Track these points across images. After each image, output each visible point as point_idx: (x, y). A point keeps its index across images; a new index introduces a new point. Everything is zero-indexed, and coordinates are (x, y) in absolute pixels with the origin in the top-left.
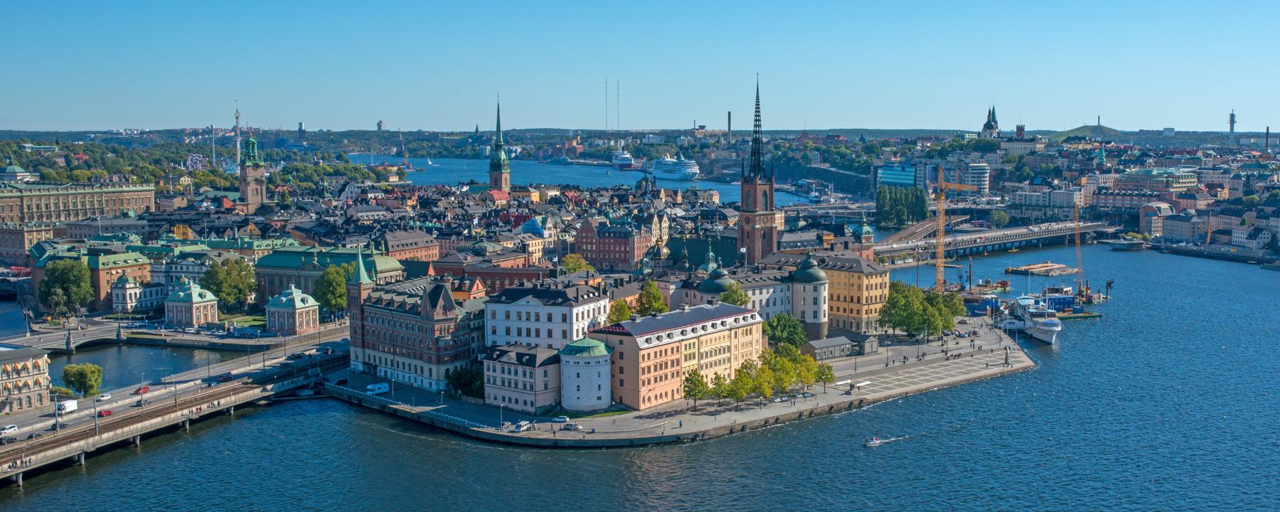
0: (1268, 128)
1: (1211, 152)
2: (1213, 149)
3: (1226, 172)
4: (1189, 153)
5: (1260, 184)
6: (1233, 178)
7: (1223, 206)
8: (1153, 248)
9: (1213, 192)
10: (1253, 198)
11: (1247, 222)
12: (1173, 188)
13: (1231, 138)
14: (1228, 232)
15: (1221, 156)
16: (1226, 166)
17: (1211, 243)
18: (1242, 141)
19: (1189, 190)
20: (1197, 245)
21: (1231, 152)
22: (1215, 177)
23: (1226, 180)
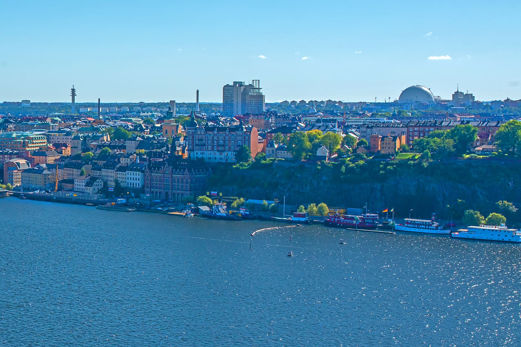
0: (99, 99)
1: (57, 118)
2: (59, 116)
3: (68, 134)
4: (40, 119)
5: (94, 143)
6: (74, 139)
7: (67, 161)
8: (15, 195)
9: (59, 150)
10: (89, 154)
11: (85, 173)
12: (29, 147)
13: (73, 107)
14: (71, 181)
15: (65, 122)
16: (68, 130)
17: (58, 190)
18: (81, 110)
19: (40, 149)
20: (48, 192)
21: (73, 118)
22: (61, 139)
23: (68, 141)
